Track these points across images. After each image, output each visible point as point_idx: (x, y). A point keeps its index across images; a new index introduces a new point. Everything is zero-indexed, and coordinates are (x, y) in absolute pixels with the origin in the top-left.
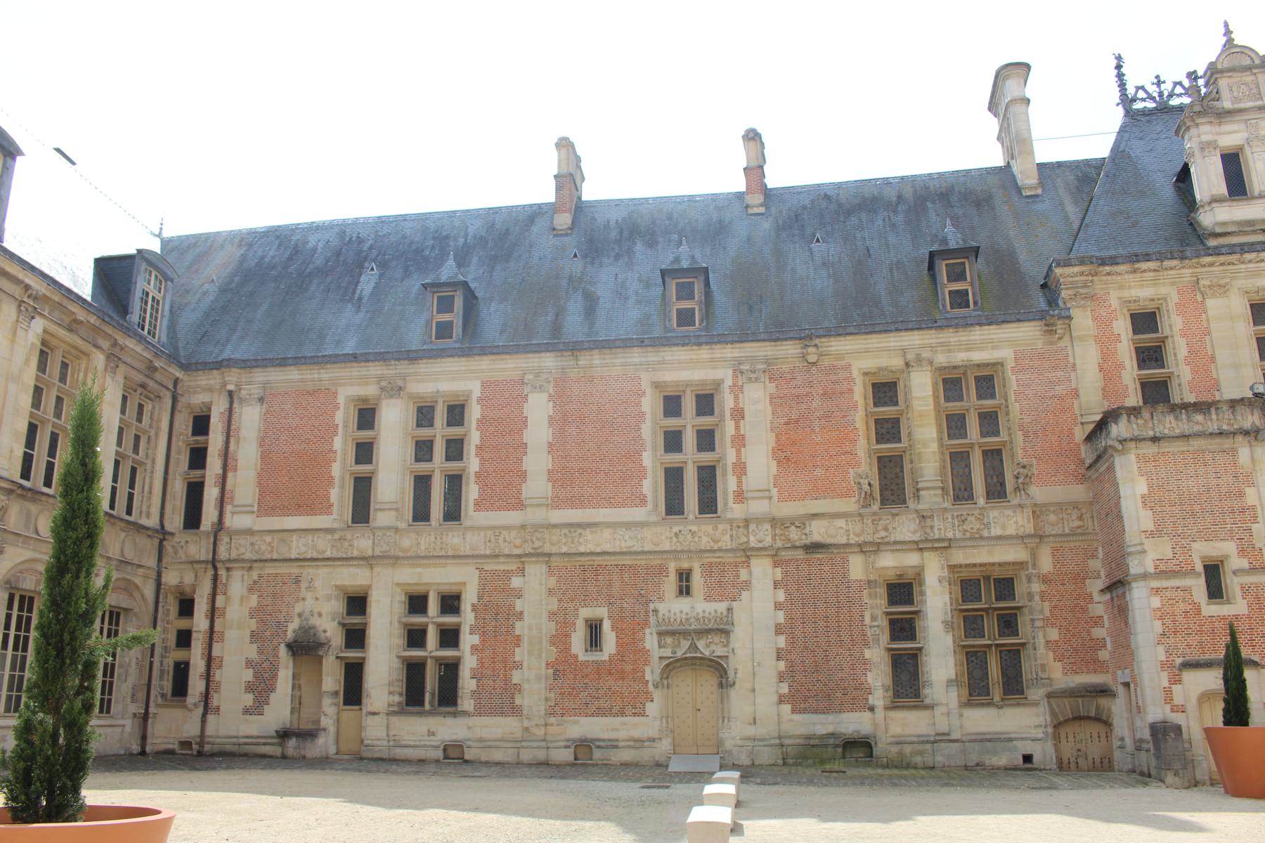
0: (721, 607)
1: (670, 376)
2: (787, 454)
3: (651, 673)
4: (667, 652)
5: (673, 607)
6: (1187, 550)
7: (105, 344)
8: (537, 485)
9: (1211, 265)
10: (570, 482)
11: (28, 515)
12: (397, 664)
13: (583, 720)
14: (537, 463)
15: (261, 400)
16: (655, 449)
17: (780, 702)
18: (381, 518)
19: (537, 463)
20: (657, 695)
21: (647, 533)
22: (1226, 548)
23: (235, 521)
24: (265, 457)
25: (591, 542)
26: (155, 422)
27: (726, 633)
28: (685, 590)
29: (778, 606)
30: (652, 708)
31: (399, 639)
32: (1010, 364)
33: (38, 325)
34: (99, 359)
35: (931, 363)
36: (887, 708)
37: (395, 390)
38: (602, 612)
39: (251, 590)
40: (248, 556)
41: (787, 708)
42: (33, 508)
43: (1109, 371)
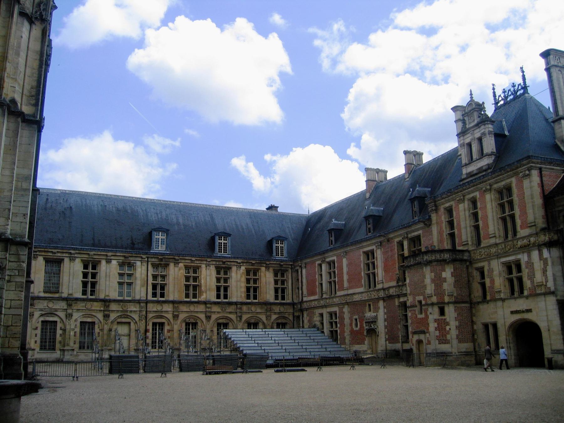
0: (375, 314)
1: (366, 249)
2: (386, 269)
3: (365, 333)
4: (367, 328)
5: (369, 315)
6: (415, 298)
7: (264, 265)
8: (346, 284)
9: (458, 192)
10: (354, 280)
11: (249, 308)
12: (329, 332)
13: (356, 346)
14: (345, 277)
15: (305, 267)
16: (364, 271)
17: (386, 341)
18: (324, 296)
19: (345, 277)
20: (367, 339)
21: (364, 295)
22: (421, 298)
23: (305, 299)
24: (307, 281)
25: (357, 298)
26: (287, 277)
27: (375, 322)
28: (370, 310)
29: (385, 313)
30: (366, 342)
31: (329, 326)
32: (422, 235)
33: (243, 268)
34: (263, 269)
35: (407, 237)
36: (402, 342)
37: (323, 261)
38: (357, 317)
39: (307, 315)
40: (307, 307)
41: (387, 342)
42: (250, 306)
43: (440, 233)
